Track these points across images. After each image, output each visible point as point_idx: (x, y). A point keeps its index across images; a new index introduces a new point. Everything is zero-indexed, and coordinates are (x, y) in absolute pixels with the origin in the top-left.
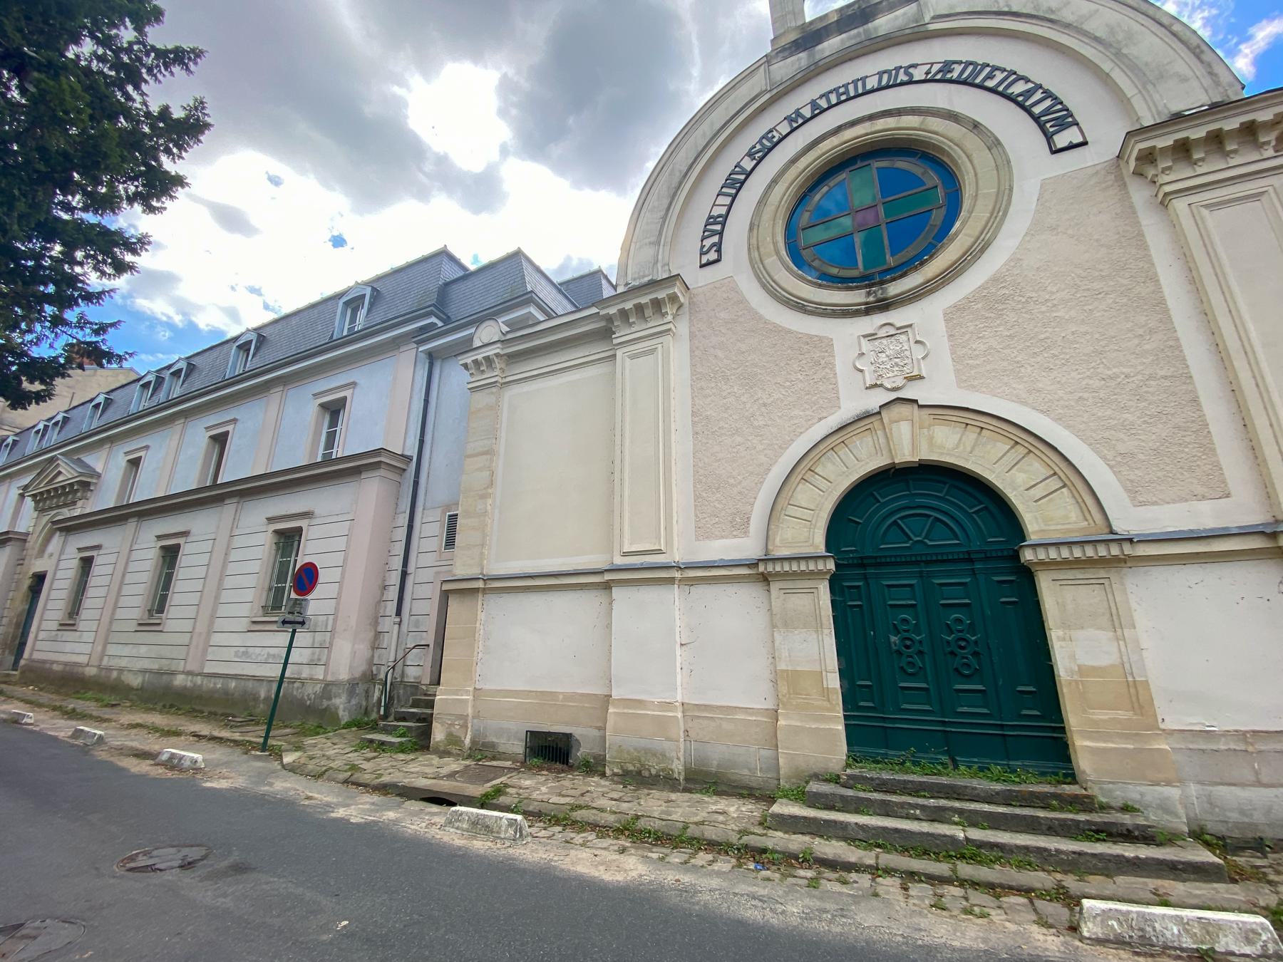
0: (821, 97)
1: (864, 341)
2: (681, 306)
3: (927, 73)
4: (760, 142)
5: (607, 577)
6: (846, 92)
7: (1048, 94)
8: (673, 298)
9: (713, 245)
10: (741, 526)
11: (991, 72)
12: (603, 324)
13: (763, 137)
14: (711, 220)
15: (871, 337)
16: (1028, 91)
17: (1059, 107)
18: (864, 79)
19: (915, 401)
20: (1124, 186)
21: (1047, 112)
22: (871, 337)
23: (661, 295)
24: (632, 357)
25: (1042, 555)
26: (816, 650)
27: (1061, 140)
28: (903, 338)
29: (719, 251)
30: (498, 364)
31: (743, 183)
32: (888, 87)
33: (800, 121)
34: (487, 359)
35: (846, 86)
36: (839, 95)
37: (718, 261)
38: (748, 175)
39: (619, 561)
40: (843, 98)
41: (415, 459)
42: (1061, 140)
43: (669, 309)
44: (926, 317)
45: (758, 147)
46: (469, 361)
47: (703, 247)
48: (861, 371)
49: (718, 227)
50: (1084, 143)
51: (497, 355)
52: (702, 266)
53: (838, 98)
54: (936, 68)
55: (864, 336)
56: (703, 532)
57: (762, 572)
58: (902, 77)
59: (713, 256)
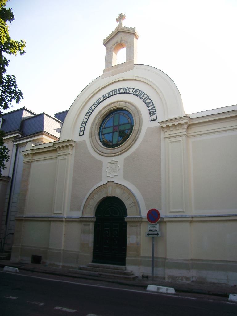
0: (111, 91)
1: (108, 164)
2: (73, 147)
3: (132, 91)
4: (96, 101)
5: (50, 219)
6: (116, 92)
7: (153, 105)
8: (71, 145)
9: (83, 130)
10: (79, 209)
11: (144, 95)
12: (55, 148)
13: (97, 100)
14: (83, 123)
15: (110, 163)
16: (149, 102)
17: (154, 108)
18: (120, 89)
19: (113, 182)
20: (160, 133)
21: (151, 109)
22: (110, 163)
23: (68, 144)
24: (61, 160)
25: (129, 220)
26: (90, 239)
27: (154, 117)
28: (116, 164)
29: (84, 132)
30: (31, 156)
31: (91, 113)
32: (124, 93)
33: (106, 98)
34: (28, 154)
35: (116, 90)
36: (114, 92)
37: (83, 135)
38: (93, 111)
39: (53, 215)
40: (115, 93)
41: (11, 178)
42: (154, 117)
43: (70, 148)
44: (120, 159)
45: (96, 103)
46: (24, 154)
47: (80, 130)
48: (107, 172)
49: (84, 125)
50: (156, 120)
51: (30, 153)
52: (80, 136)
53: (114, 93)
54: (135, 90)
55: (109, 163)
56: (72, 209)
57: (82, 220)
58: (128, 91)
59: (82, 133)
